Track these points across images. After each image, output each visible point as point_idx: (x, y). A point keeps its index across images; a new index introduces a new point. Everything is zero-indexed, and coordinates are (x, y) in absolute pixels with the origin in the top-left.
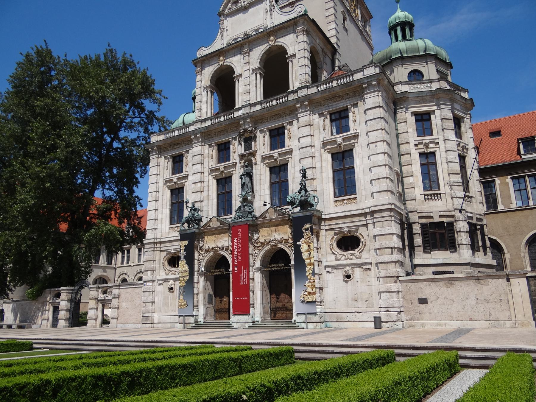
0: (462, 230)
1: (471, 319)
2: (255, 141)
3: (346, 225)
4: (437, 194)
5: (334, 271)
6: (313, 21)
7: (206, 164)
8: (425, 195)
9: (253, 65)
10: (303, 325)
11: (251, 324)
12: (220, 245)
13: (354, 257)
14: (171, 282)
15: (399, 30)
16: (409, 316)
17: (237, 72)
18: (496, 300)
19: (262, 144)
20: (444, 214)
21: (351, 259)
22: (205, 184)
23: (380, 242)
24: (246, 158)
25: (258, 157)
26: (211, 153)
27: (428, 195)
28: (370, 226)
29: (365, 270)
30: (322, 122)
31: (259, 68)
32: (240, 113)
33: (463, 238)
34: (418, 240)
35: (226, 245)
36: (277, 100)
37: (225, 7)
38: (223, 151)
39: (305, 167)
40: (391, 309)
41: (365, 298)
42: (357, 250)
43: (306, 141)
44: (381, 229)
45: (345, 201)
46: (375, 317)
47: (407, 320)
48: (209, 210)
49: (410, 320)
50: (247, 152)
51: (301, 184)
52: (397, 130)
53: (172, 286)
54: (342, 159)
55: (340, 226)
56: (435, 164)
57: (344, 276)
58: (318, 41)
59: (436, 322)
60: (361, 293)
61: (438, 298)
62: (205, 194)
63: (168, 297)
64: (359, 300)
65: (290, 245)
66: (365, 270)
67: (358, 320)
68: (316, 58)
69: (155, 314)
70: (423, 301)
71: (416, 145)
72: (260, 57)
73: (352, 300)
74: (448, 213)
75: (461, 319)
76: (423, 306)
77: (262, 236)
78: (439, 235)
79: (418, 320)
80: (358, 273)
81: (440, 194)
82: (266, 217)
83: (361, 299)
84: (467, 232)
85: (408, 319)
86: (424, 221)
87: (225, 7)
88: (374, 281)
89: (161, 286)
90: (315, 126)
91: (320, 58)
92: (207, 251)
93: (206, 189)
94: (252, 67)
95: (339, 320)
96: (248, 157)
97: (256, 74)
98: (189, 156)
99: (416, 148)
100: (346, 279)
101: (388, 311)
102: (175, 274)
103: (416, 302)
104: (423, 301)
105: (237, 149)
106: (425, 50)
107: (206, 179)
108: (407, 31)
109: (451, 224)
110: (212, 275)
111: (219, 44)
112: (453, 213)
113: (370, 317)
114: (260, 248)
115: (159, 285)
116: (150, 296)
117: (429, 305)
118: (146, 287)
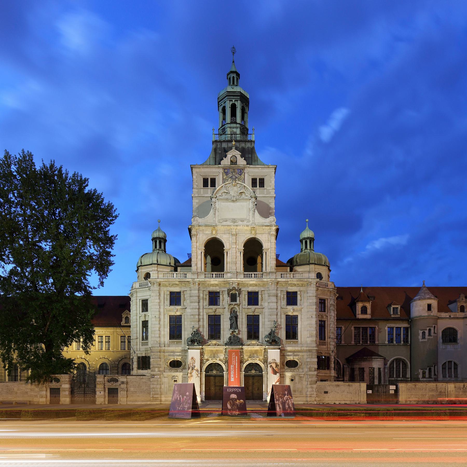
7: (201, 304)
22: (201, 317)
25: (241, 307)
30: (282, 296)
50: (234, 303)
51: (272, 330)
62: (201, 323)
70: (326, 392)
76: (326, 395)
83: (298, 391)
88: (305, 383)
90: (279, 298)
93: (201, 320)
104: (326, 392)
105: (225, 299)
107: (201, 314)
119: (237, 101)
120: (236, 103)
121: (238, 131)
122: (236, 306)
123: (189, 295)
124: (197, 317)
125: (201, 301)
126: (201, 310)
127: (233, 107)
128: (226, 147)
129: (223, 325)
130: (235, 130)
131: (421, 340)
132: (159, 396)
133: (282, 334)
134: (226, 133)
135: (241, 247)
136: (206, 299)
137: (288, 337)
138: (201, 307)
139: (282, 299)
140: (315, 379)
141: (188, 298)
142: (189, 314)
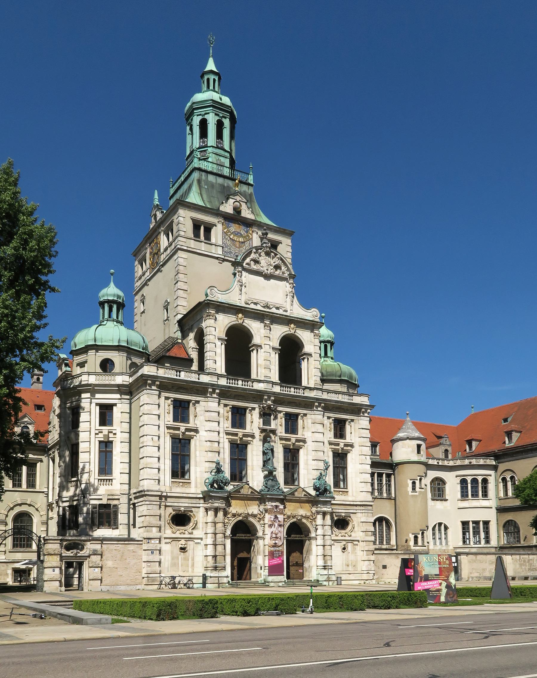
5: (335, 544)
9: (272, 341)
10: (325, 583)
13: (346, 535)
14: (183, 542)
17: (256, 340)
19: (278, 424)
21: (345, 536)
26: (226, 414)
28: (359, 515)
29: (354, 545)
35: (256, 512)
38: (238, 417)
41: (354, 564)
43: (319, 437)
45: (341, 493)
51: (321, 474)
53: (186, 546)
54: (340, 458)
55: (340, 511)
63: (178, 558)
65: (310, 520)
66: (354, 545)
70: (385, 567)
89: (168, 545)
92: (234, 515)
98: (200, 408)
101: (368, 573)
102: (184, 534)
104: (385, 567)
115: (166, 543)
119: (225, 118)
121: (227, 163)
123: (203, 408)
126: (221, 435)
128: (214, 181)
129: (252, 461)
130: (222, 159)
131: (410, 494)
132: (158, 575)
133: (330, 479)
134: (210, 160)
137: (336, 484)
138: (222, 431)
141: (202, 412)
142: (204, 439)
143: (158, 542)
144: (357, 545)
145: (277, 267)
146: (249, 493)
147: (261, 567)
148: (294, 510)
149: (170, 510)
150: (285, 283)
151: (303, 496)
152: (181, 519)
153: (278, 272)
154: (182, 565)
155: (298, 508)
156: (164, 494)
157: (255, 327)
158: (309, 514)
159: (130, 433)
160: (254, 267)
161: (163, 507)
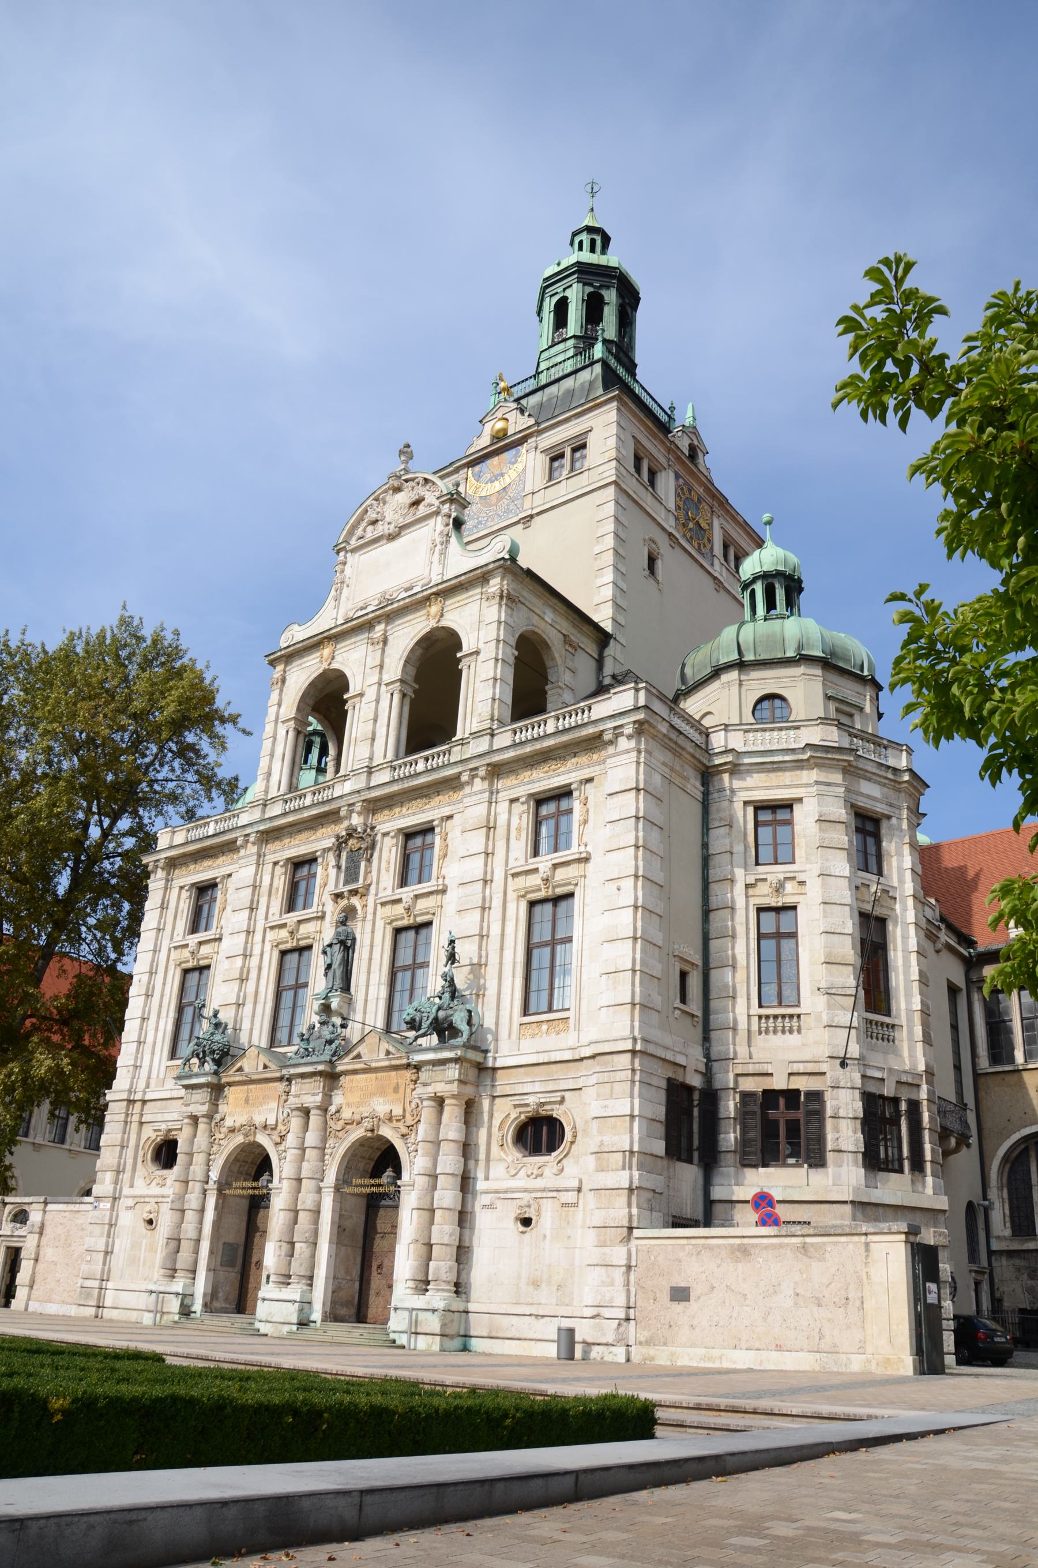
0: (842, 1113)
1: (779, 1348)
2: (369, 861)
3: (537, 1087)
4: (791, 1016)
5: (499, 1204)
6: (529, 573)
8: (760, 1017)
11: (294, 1328)
12: (259, 1120)
15: (759, 588)
16: (646, 1333)
18: (836, 1299)
20: (801, 1068)
22: (254, 962)
23: (600, 1138)
24: (343, 903)
25: (371, 899)
27: (767, 1017)
28: (589, 1094)
29: (565, 1205)
31: (401, 681)
32: (348, 787)
33: (844, 1134)
34: (730, 1137)
36: (427, 759)
37: (351, 533)
39: (456, 935)
40: (606, 1313)
42: (554, 1154)
44: (606, 1102)
45: (544, 1027)
46: (559, 1329)
47: (641, 1343)
48: (253, 1029)
49: (648, 1343)
52: (705, 846)
53: (151, 1216)
56: (793, 935)
57: (517, 1219)
58: (549, 616)
59: (703, 1351)
60: (550, 1265)
61: (713, 1288)
62: (251, 986)
63: (141, 1244)
64: (544, 1285)
67: (534, 1337)
68: (545, 658)
69: (110, 1285)
70: (680, 1295)
71: (748, 886)
72: (406, 654)
73: (528, 1284)
74: (810, 1068)
75: (757, 1345)
76: (678, 1307)
77: (348, 1105)
78: (785, 1126)
79: (665, 1344)
80: (547, 1219)
81: (799, 1016)
82: (359, 1056)
84: (855, 1118)
85: (643, 1339)
86: (749, 1085)
87: (351, 533)
89: (130, 1213)
90: (501, 831)
91: (553, 659)
92: (232, 1130)
93: (253, 975)
94: (387, 678)
95: (494, 1334)
96: (349, 899)
97: (392, 694)
99: (751, 892)
100: (522, 1228)
103: (666, 1295)
104: (680, 1295)
106: (800, 647)
108: (780, 595)
109: (816, 1096)
110: (241, 1196)
111: (325, 620)
112: (824, 1067)
113: (550, 1329)
114: (340, 1134)
115: (129, 1208)
116: (102, 1235)
117: (693, 1305)
118: (96, 1213)
120: (568, 293)
122: (355, 901)
124: (239, 961)
125: (264, 901)
126: (258, 937)
127: (561, 309)
135: (394, 669)
136: (278, 889)
139: (513, 833)
140: (619, 1211)
143: (109, 1205)
144: (575, 1205)
145: (416, 503)
146: (261, 1068)
147: (268, 1277)
148: (360, 1104)
149: (148, 1132)
150: (431, 522)
151: (382, 1055)
152: (166, 1153)
153: (422, 510)
154: (144, 1264)
155: (372, 1094)
156: (138, 1096)
157: (354, 660)
158: (398, 1111)
159: (856, 996)
160: (371, 533)
161: (135, 1126)
